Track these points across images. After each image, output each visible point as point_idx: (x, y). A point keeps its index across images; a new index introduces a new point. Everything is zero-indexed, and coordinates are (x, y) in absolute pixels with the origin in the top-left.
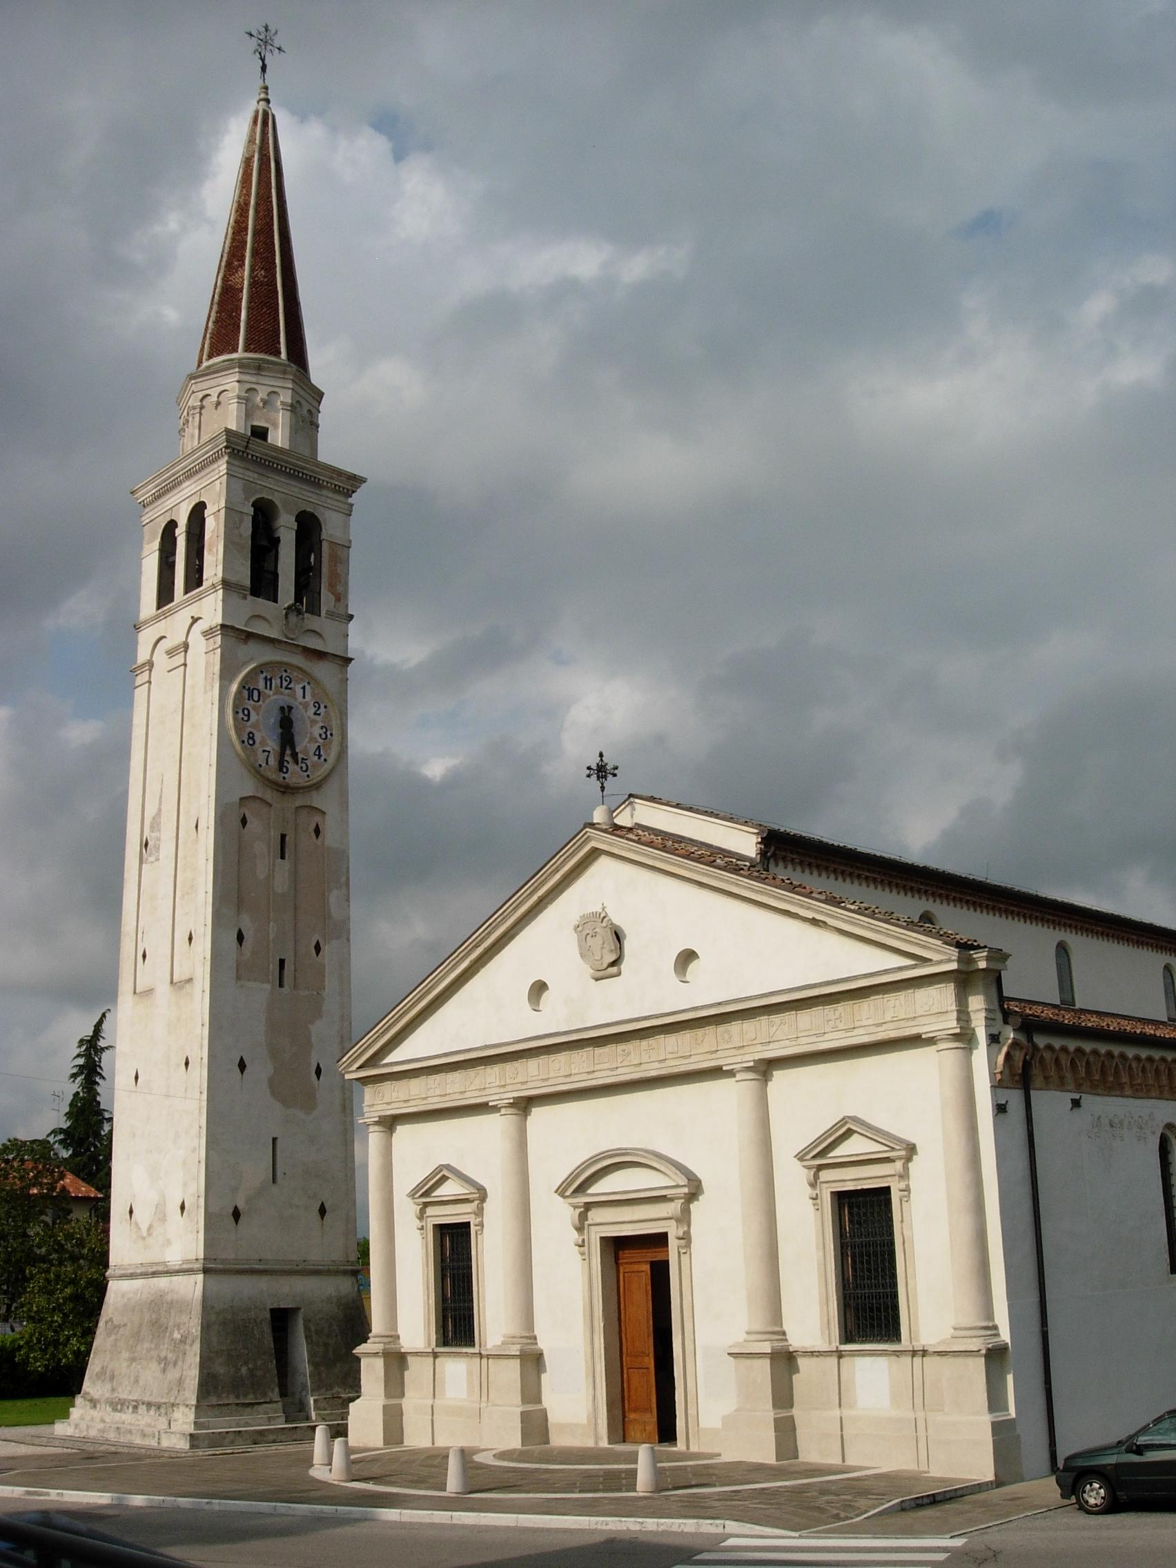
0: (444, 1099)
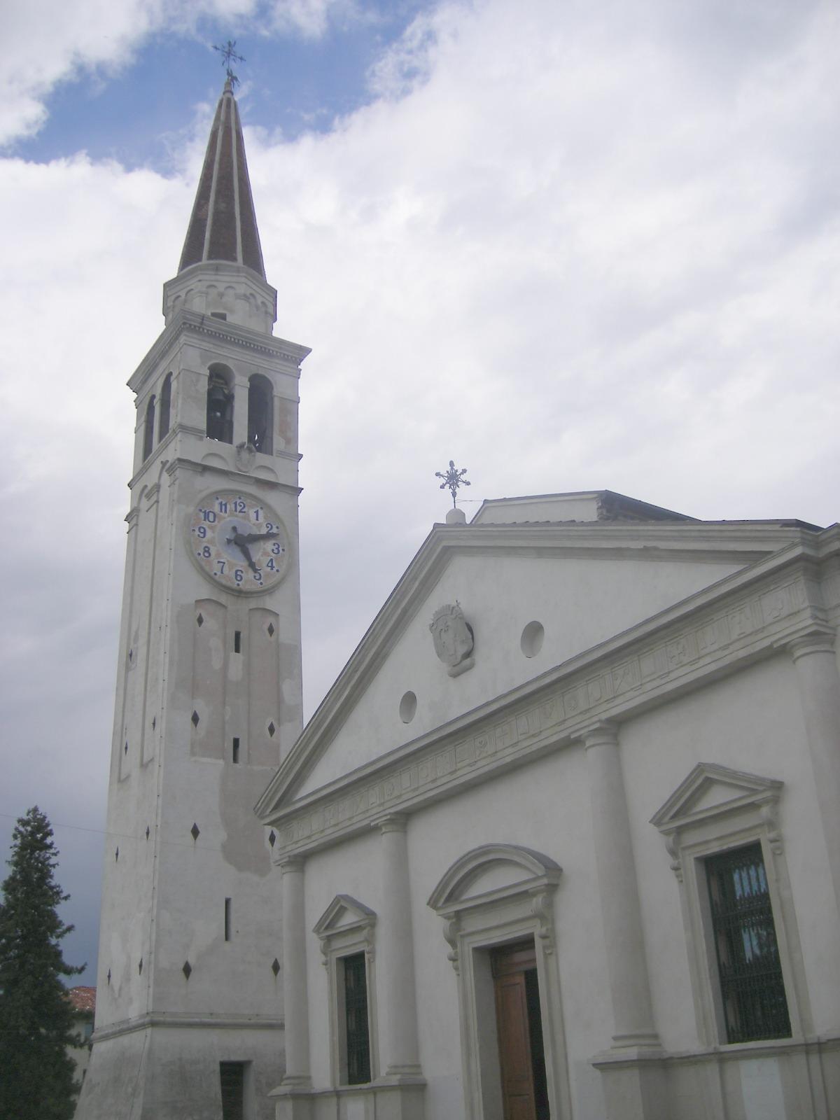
0: (337, 828)
